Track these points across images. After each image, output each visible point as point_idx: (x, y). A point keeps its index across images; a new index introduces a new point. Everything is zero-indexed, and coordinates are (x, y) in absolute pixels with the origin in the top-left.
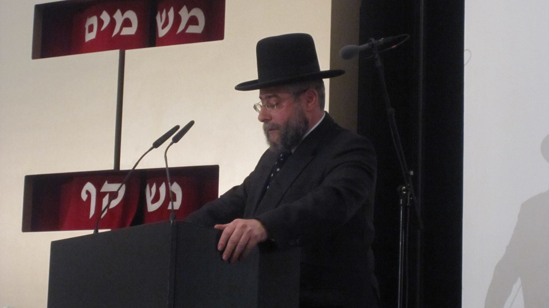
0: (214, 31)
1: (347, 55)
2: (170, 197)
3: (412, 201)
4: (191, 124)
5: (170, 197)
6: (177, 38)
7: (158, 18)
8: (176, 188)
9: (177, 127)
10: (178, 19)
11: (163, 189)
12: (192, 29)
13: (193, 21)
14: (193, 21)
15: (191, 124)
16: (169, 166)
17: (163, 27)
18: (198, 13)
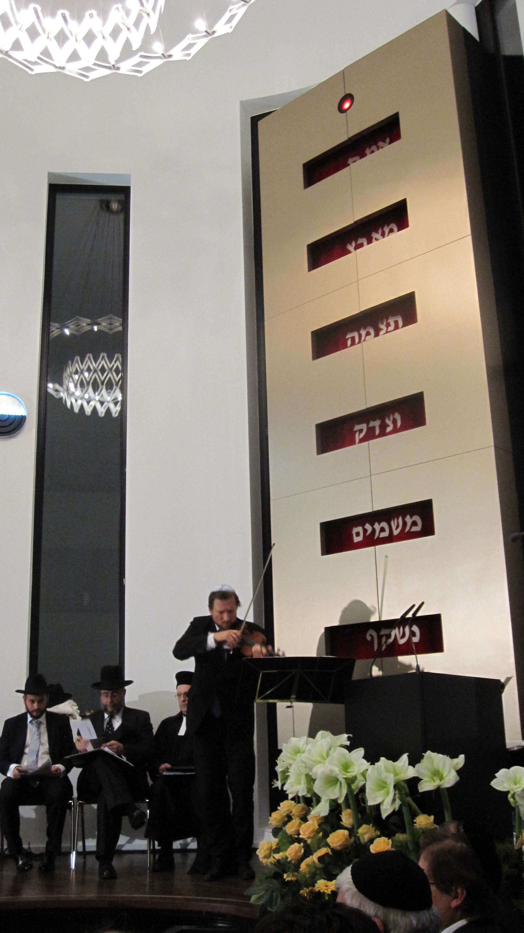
0: (428, 529)
1: (514, 540)
2: (413, 634)
4: (423, 603)
5: (413, 634)
6: (405, 535)
7: (392, 523)
8: (415, 629)
9: (413, 606)
10: (405, 524)
11: (407, 629)
12: (415, 529)
13: (414, 524)
14: (414, 524)
15: (423, 603)
16: (414, 656)
17: (397, 528)
18: (417, 518)
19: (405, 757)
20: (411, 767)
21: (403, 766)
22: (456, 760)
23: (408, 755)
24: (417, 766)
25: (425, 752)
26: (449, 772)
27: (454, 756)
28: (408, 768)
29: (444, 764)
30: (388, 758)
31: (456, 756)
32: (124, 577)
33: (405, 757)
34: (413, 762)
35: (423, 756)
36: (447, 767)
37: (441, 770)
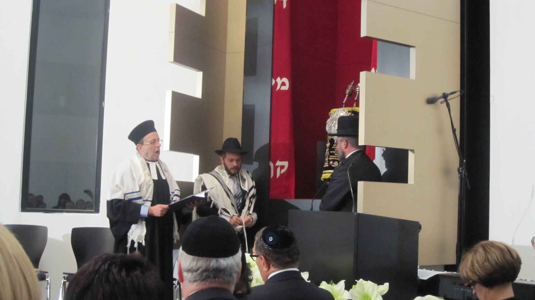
3: (465, 175)
19: (342, 283)
20: (346, 291)
21: (340, 290)
22: (381, 286)
23: (345, 282)
24: (351, 290)
25: (358, 280)
26: (377, 297)
27: (380, 282)
28: (343, 293)
29: (373, 291)
30: (328, 282)
31: (383, 284)
32: (104, 101)
33: (342, 283)
34: (348, 287)
35: (356, 283)
36: (375, 293)
37: (370, 294)
